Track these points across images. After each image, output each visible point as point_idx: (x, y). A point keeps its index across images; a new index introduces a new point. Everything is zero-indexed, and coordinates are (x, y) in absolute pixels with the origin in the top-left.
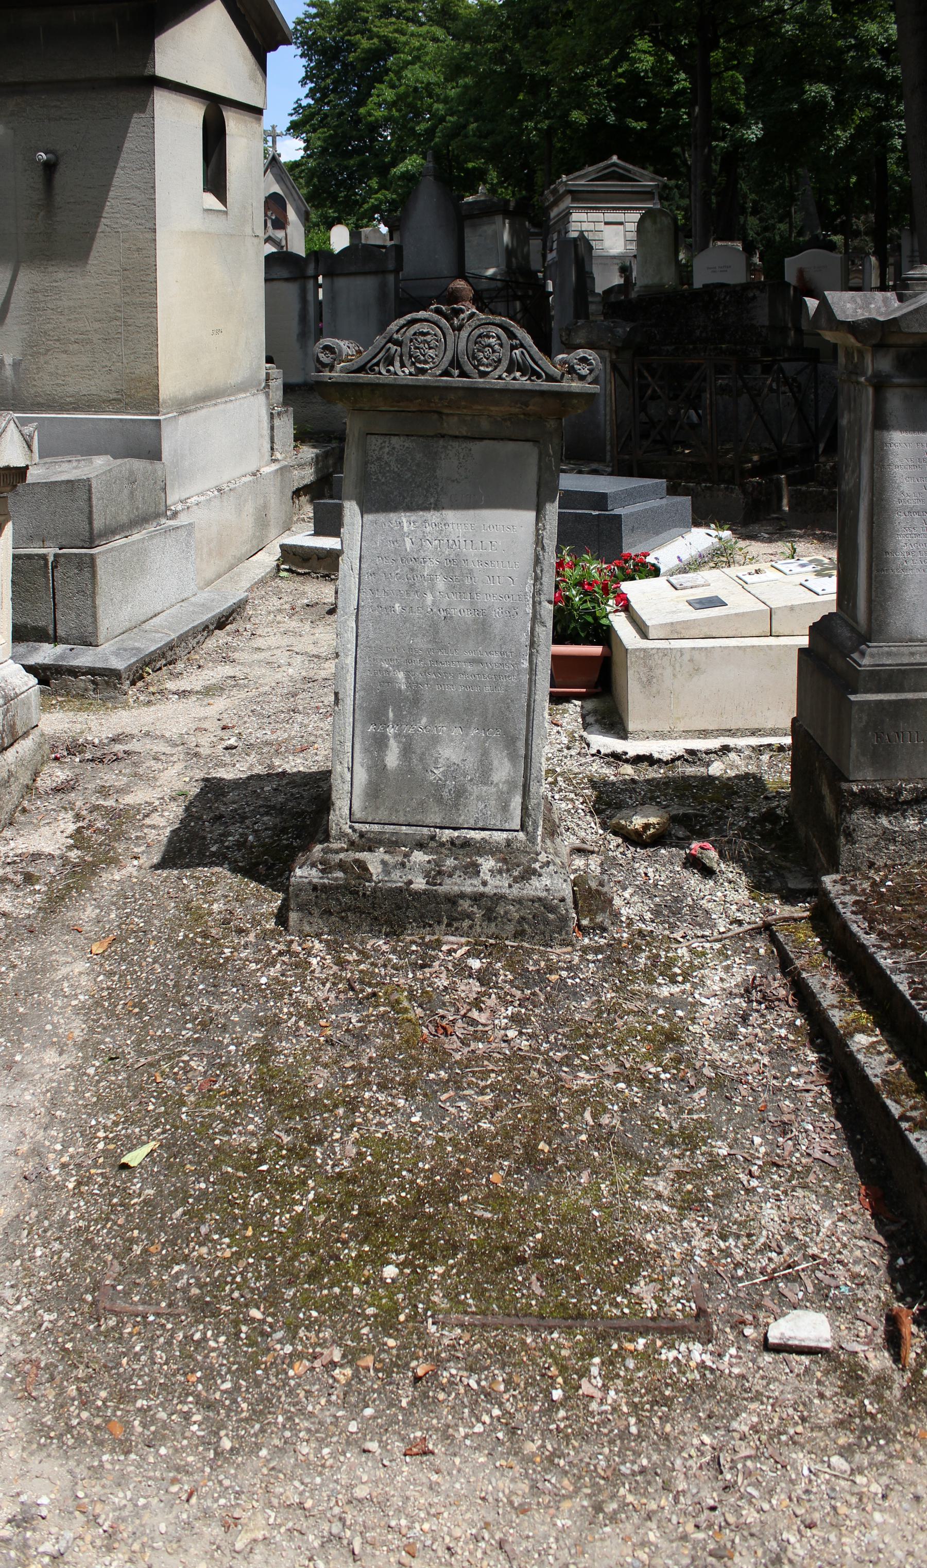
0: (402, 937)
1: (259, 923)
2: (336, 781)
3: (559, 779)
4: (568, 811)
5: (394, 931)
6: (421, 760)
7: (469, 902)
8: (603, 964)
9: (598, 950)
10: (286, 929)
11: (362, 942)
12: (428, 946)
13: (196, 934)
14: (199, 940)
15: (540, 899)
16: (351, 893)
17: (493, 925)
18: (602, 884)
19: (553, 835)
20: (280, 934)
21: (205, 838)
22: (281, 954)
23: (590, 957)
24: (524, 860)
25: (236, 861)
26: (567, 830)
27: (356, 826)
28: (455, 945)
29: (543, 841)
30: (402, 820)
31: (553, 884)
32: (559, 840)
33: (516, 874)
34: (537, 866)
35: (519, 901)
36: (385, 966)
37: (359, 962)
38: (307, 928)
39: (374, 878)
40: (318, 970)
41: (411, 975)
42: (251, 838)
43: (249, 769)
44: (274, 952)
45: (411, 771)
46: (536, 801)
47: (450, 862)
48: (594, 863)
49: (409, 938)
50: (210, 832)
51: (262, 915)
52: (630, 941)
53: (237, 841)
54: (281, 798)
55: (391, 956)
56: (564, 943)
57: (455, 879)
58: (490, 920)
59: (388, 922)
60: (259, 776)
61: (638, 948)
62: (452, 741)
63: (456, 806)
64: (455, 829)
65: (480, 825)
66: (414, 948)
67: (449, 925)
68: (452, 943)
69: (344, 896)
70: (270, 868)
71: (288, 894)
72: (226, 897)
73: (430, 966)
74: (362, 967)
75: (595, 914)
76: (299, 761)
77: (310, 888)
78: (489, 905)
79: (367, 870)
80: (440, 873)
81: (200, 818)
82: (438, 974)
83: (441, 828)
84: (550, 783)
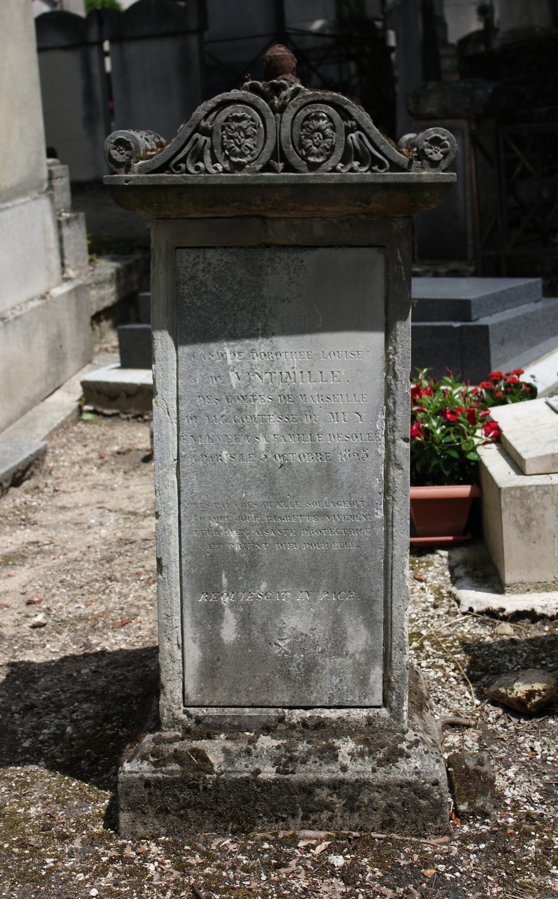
0: (251, 835)
1: (85, 827)
2: (165, 661)
3: (426, 643)
4: (438, 680)
5: (242, 827)
6: (263, 631)
7: (327, 791)
8: (486, 855)
9: (479, 838)
10: (117, 832)
11: (206, 842)
12: (283, 842)
13: (12, 844)
14: (16, 850)
15: (409, 784)
16: (189, 787)
17: (356, 815)
18: (480, 763)
19: (421, 709)
20: (110, 838)
21: (15, 732)
22: (112, 860)
23: (471, 847)
24: (389, 739)
25: (53, 757)
26: (438, 702)
27: (192, 710)
28: (313, 840)
29: (410, 717)
30: (244, 701)
31: (423, 765)
32: (428, 715)
33: (380, 756)
34: (404, 746)
35: (385, 787)
36: (233, 868)
37: (203, 866)
38: (141, 830)
39: (216, 768)
40: (157, 877)
41: (264, 878)
42: (69, 729)
43: (62, 649)
44: (104, 859)
45: (251, 645)
46: (399, 672)
47: (303, 747)
48: (471, 739)
49: (259, 835)
50: (22, 725)
51: (88, 817)
52: (516, 827)
53: (54, 733)
54: (101, 682)
55: (240, 857)
56: (439, 833)
57: (310, 765)
58: (352, 810)
59: (235, 818)
60: (74, 658)
61: (527, 835)
62: (298, 608)
63: (306, 682)
64: (306, 708)
65: (336, 702)
66: (266, 846)
67: (305, 818)
68: (311, 838)
69: (181, 791)
70: (95, 762)
71: (116, 792)
72: (45, 799)
73: (286, 866)
74: (207, 870)
75: (475, 797)
76: (120, 637)
77: (141, 784)
78: (351, 793)
79: (207, 760)
80: (292, 759)
81: (8, 710)
82: (295, 874)
83: (290, 708)
84: (416, 649)
